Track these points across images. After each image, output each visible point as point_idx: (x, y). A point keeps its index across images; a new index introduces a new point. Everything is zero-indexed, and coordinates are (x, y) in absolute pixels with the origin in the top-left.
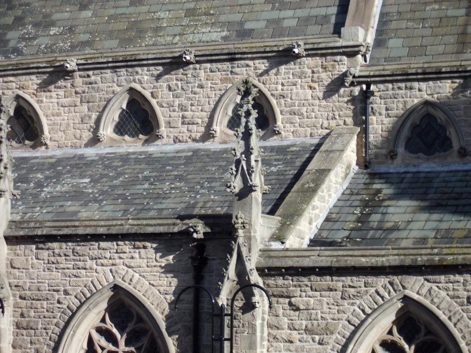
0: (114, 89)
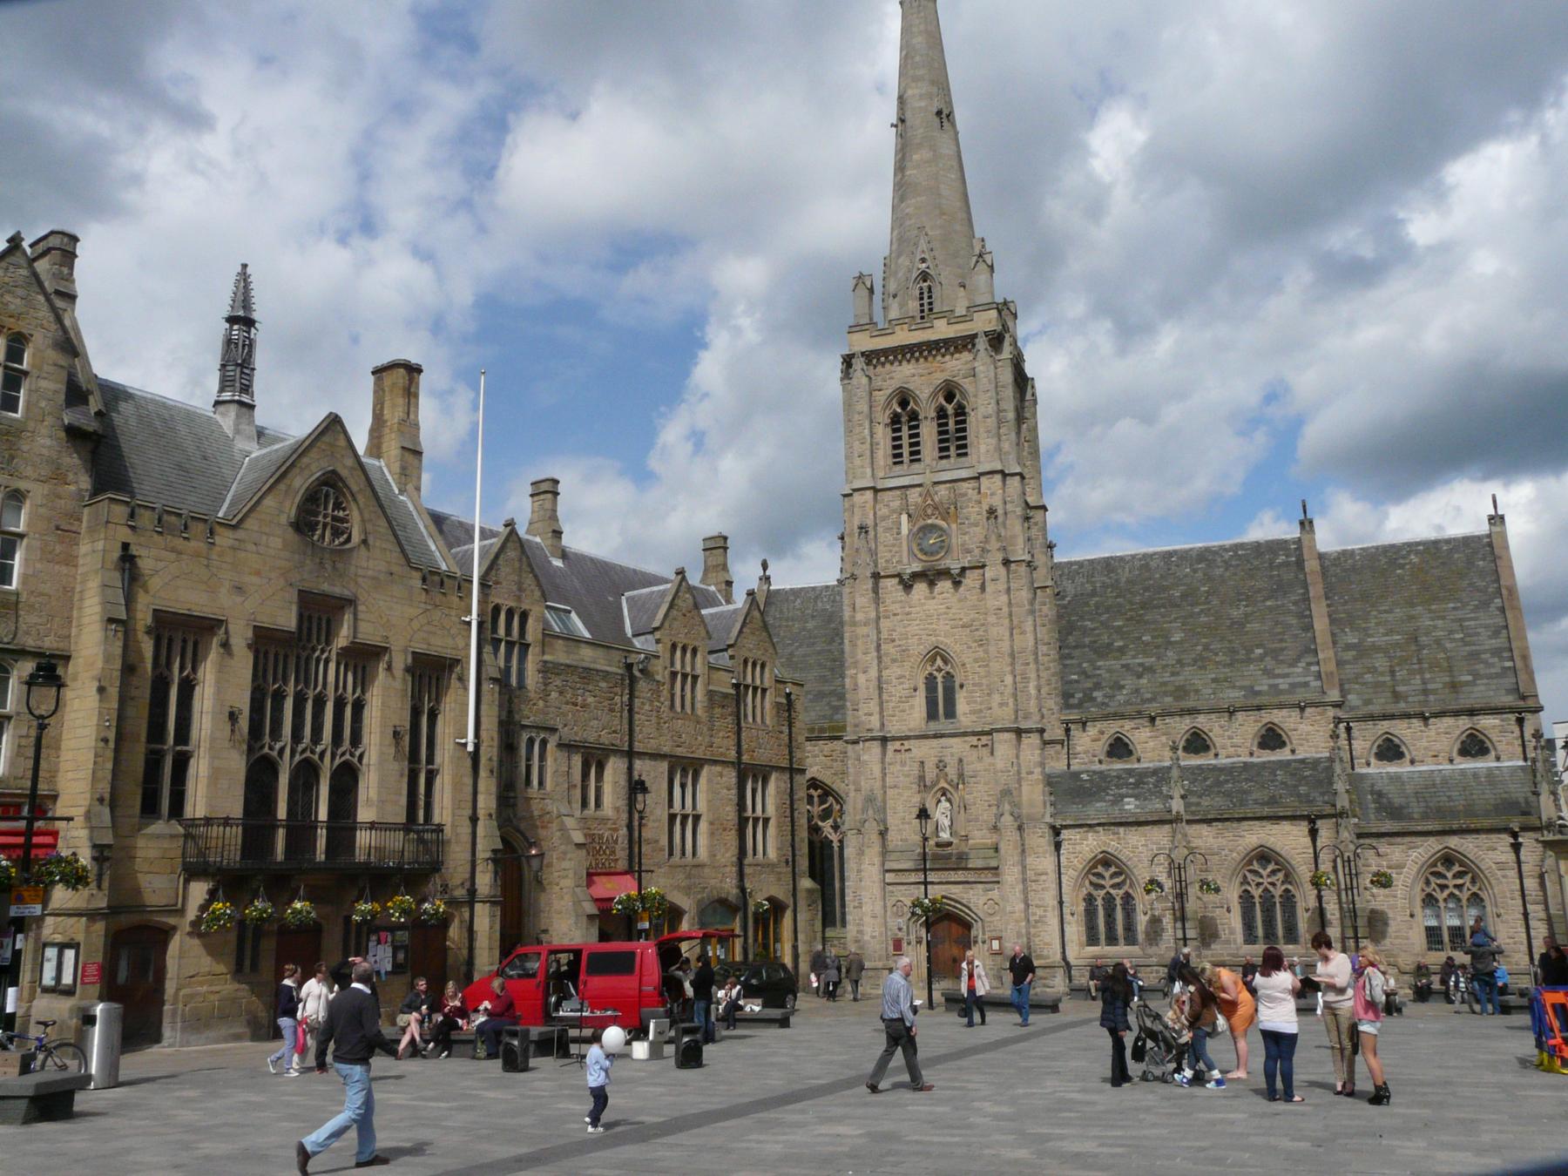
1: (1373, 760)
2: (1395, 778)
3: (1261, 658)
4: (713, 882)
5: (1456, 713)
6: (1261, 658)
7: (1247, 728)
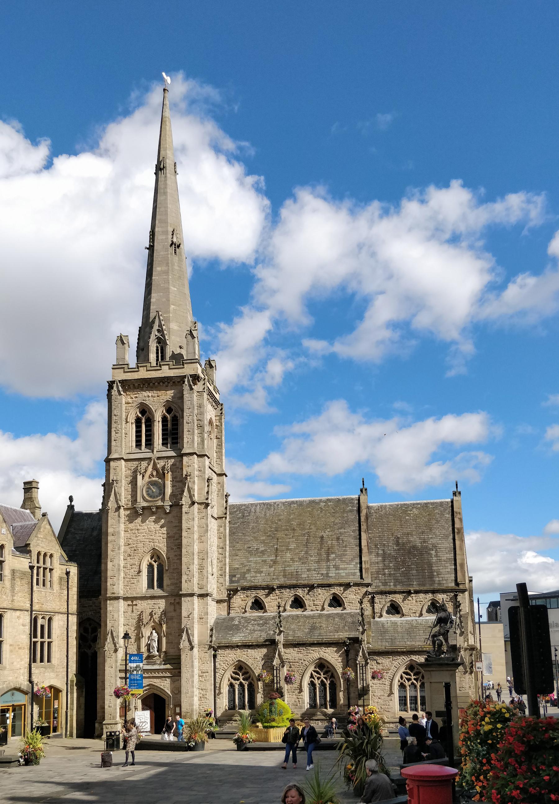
0: (288, 595)
1: (384, 614)
2: (395, 623)
3: (334, 559)
4: (10, 678)
5: (426, 592)
6: (334, 559)
7: (324, 596)
